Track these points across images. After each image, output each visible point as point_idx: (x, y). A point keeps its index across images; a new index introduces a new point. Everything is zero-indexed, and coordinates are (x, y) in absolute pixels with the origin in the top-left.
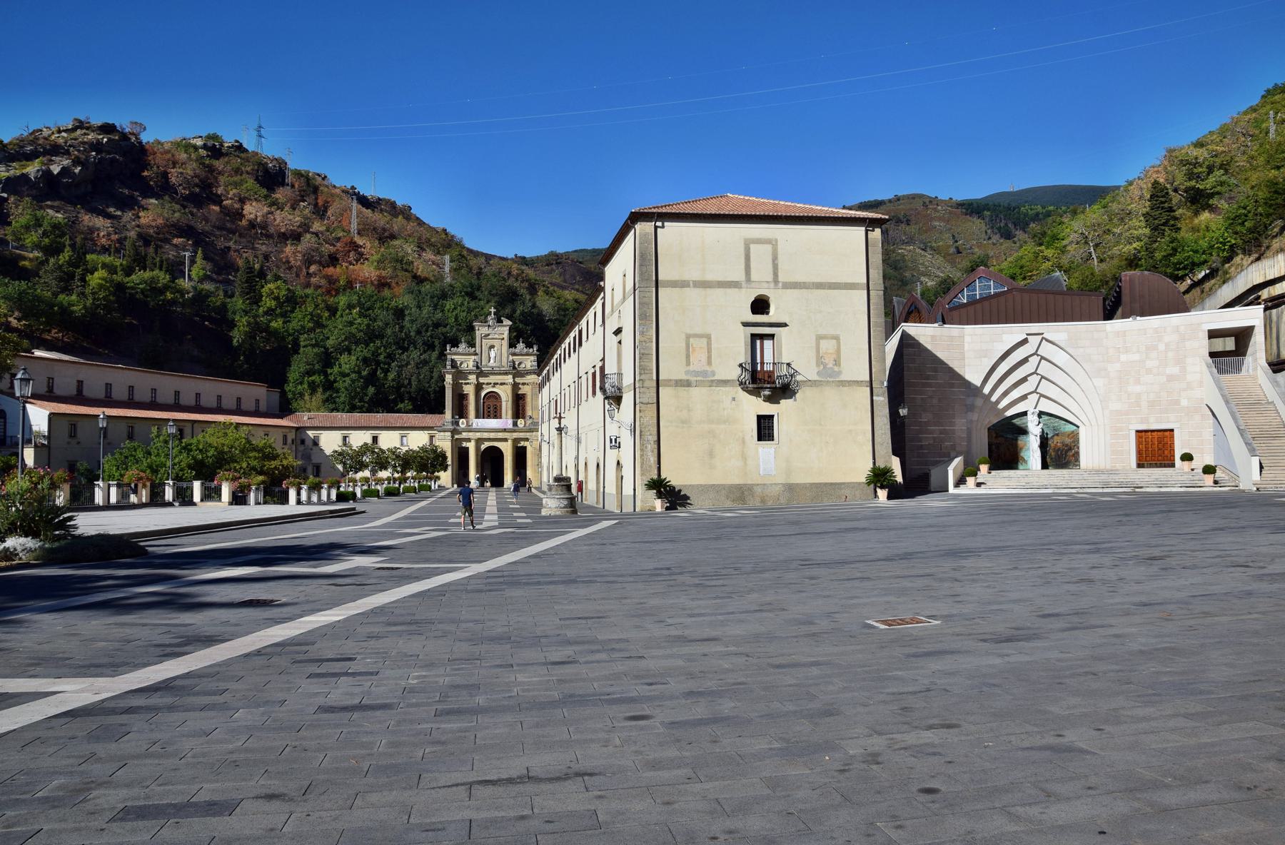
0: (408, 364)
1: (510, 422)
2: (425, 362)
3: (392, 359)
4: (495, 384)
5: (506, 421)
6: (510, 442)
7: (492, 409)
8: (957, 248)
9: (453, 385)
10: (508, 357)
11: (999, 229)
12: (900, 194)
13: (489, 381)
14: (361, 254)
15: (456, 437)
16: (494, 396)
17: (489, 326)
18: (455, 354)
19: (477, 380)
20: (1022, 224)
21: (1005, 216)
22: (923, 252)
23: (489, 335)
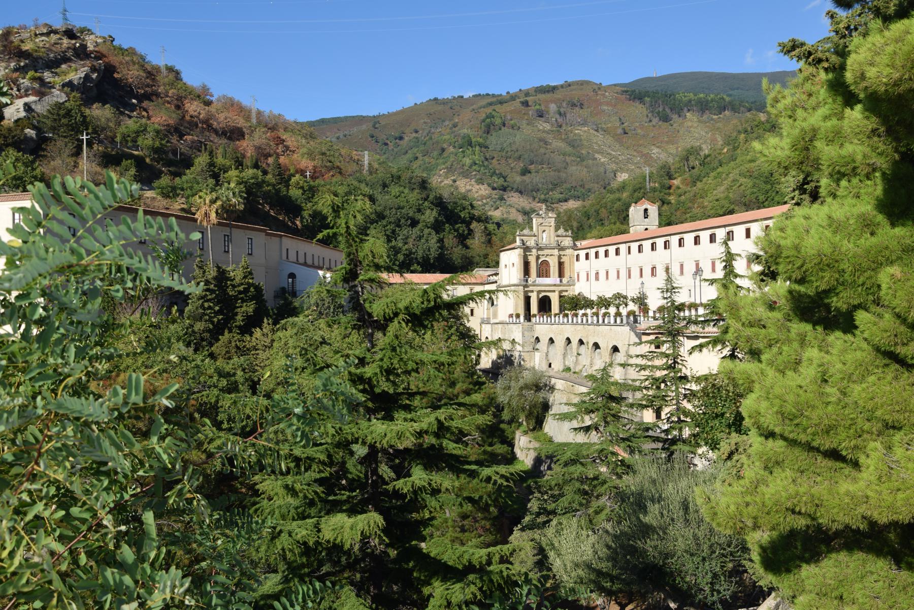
1: (558, 279)
5: (553, 279)
6: (557, 293)
8: (624, 129)
11: (658, 113)
12: (570, 80)
14: (287, 148)
16: (546, 263)
18: (523, 235)
20: (679, 109)
21: (663, 102)
22: (596, 133)
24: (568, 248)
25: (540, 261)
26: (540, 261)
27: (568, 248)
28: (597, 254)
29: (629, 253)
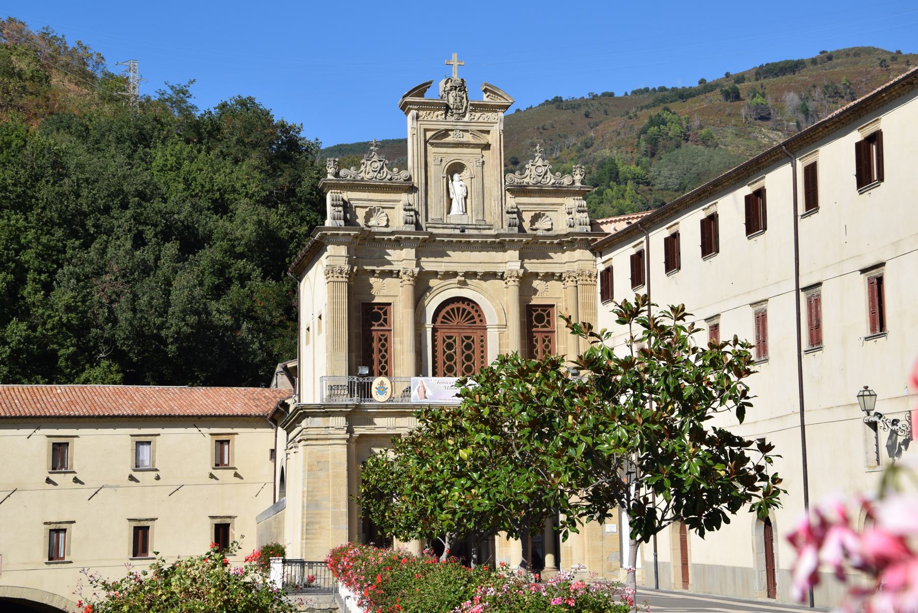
0: (99, 272)
2: (147, 270)
3: (56, 262)
4: (472, 275)
7: (458, 347)
9: (350, 274)
10: (502, 199)
12: (831, 48)
13: (452, 268)
15: (359, 430)
17: (447, 108)
19: (418, 264)
23: (446, 133)
24: (566, 243)
25: (431, 305)
26: (431, 307)
27: (566, 243)
28: (672, 245)
29: (812, 202)
